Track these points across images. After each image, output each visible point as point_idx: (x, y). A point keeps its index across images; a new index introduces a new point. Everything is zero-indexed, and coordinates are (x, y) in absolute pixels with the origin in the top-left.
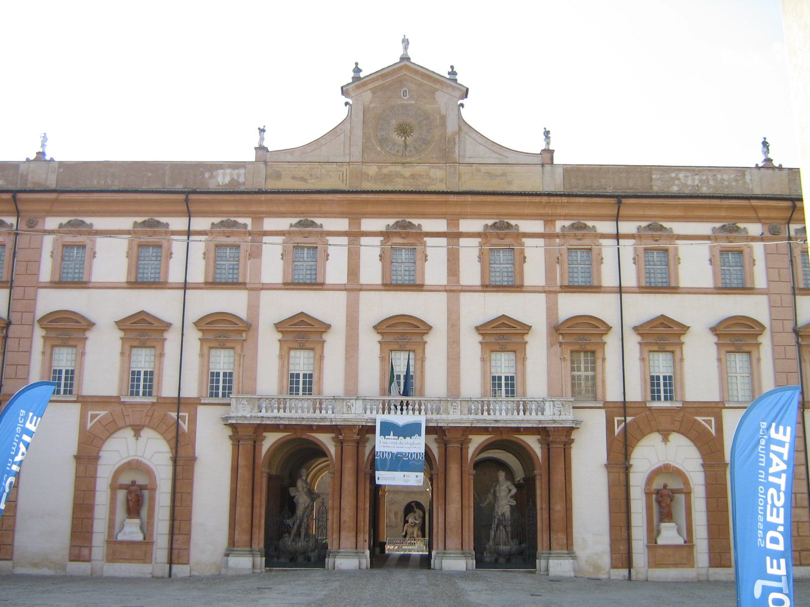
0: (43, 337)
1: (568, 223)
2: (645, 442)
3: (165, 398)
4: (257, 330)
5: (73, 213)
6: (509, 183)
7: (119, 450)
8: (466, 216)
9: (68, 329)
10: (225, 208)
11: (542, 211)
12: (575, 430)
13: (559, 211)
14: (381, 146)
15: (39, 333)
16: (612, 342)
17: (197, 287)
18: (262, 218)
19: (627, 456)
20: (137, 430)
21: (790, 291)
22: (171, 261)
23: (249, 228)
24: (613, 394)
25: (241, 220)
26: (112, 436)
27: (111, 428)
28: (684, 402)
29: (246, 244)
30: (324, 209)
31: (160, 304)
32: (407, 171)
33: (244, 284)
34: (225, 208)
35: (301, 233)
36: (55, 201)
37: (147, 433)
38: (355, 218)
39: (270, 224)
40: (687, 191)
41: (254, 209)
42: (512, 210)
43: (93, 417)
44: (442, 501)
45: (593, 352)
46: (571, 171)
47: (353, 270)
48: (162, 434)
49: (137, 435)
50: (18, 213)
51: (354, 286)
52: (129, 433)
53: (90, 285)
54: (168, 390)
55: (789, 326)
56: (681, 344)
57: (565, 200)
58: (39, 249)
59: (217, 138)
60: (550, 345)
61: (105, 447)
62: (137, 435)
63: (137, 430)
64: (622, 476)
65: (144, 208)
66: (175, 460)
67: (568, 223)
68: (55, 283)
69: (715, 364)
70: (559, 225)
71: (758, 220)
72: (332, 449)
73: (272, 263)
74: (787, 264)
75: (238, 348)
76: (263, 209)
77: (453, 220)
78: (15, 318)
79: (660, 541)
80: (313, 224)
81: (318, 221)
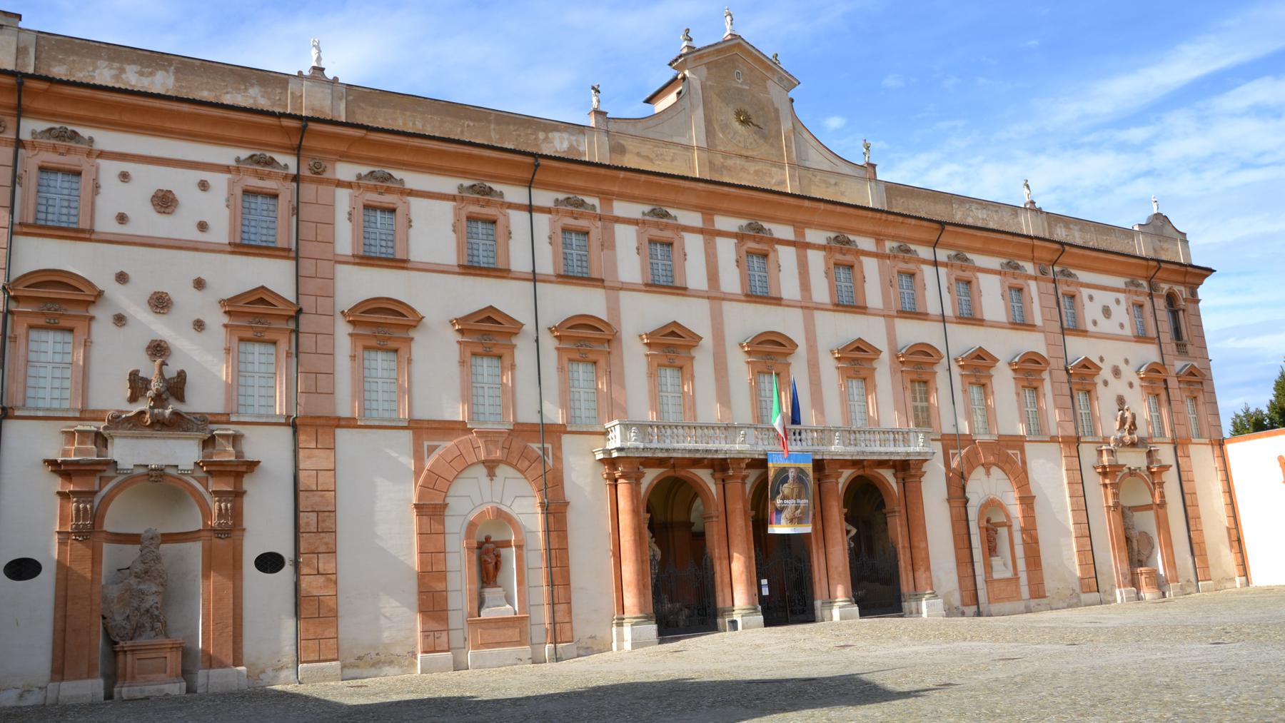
0: (351, 335)
1: (895, 244)
2: (973, 476)
3: (522, 424)
4: (620, 340)
5: (378, 161)
6: (842, 193)
7: (471, 498)
8: (810, 225)
9: (386, 325)
10: (572, 182)
11: (877, 229)
12: (925, 464)
13: (892, 231)
14: (723, 133)
15: (343, 330)
16: (941, 371)
17: (546, 280)
18: (611, 200)
19: (964, 489)
20: (491, 467)
21: (1059, 331)
22: (511, 242)
23: (598, 211)
24: (948, 429)
25: (589, 200)
26: (462, 475)
27: (461, 466)
28: (1000, 436)
29: (596, 229)
30: (681, 198)
31: (507, 298)
32: (752, 167)
33: (603, 281)
34: (572, 182)
35: (657, 225)
36: (361, 139)
37: (503, 471)
38: (708, 212)
39: (620, 208)
40: (979, 225)
41: (605, 187)
42: (854, 224)
43: (432, 449)
44: (822, 545)
45: (925, 382)
46: (893, 189)
47: (713, 276)
48: (522, 472)
49: (491, 475)
50: (297, 151)
51: (715, 296)
52: (482, 471)
53: (409, 265)
54: (528, 415)
55: (1062, 364)
56: (991, 377)
57: (900, 219)
58: (331, 206)
59: (544, 89)
60: (893, 372)
61: (452, 492)
62: (491, 475)
63: (491, 467)
64: (962, 510)
65: (473, 167)
66: (546, 508)
67: (895, 244)
68: (362, 257)
69: (1014, 397)
70: (889, 245)
71: (1033, 260)
72: (713, 487)
73: (628, 259)
74: (1054, 305)
75: (602, 362)
76: (616, 189)
77: (800, 227)
78: (306, 303)
79: (996, 576)
80: (666, 215)
81: (672, 212)
